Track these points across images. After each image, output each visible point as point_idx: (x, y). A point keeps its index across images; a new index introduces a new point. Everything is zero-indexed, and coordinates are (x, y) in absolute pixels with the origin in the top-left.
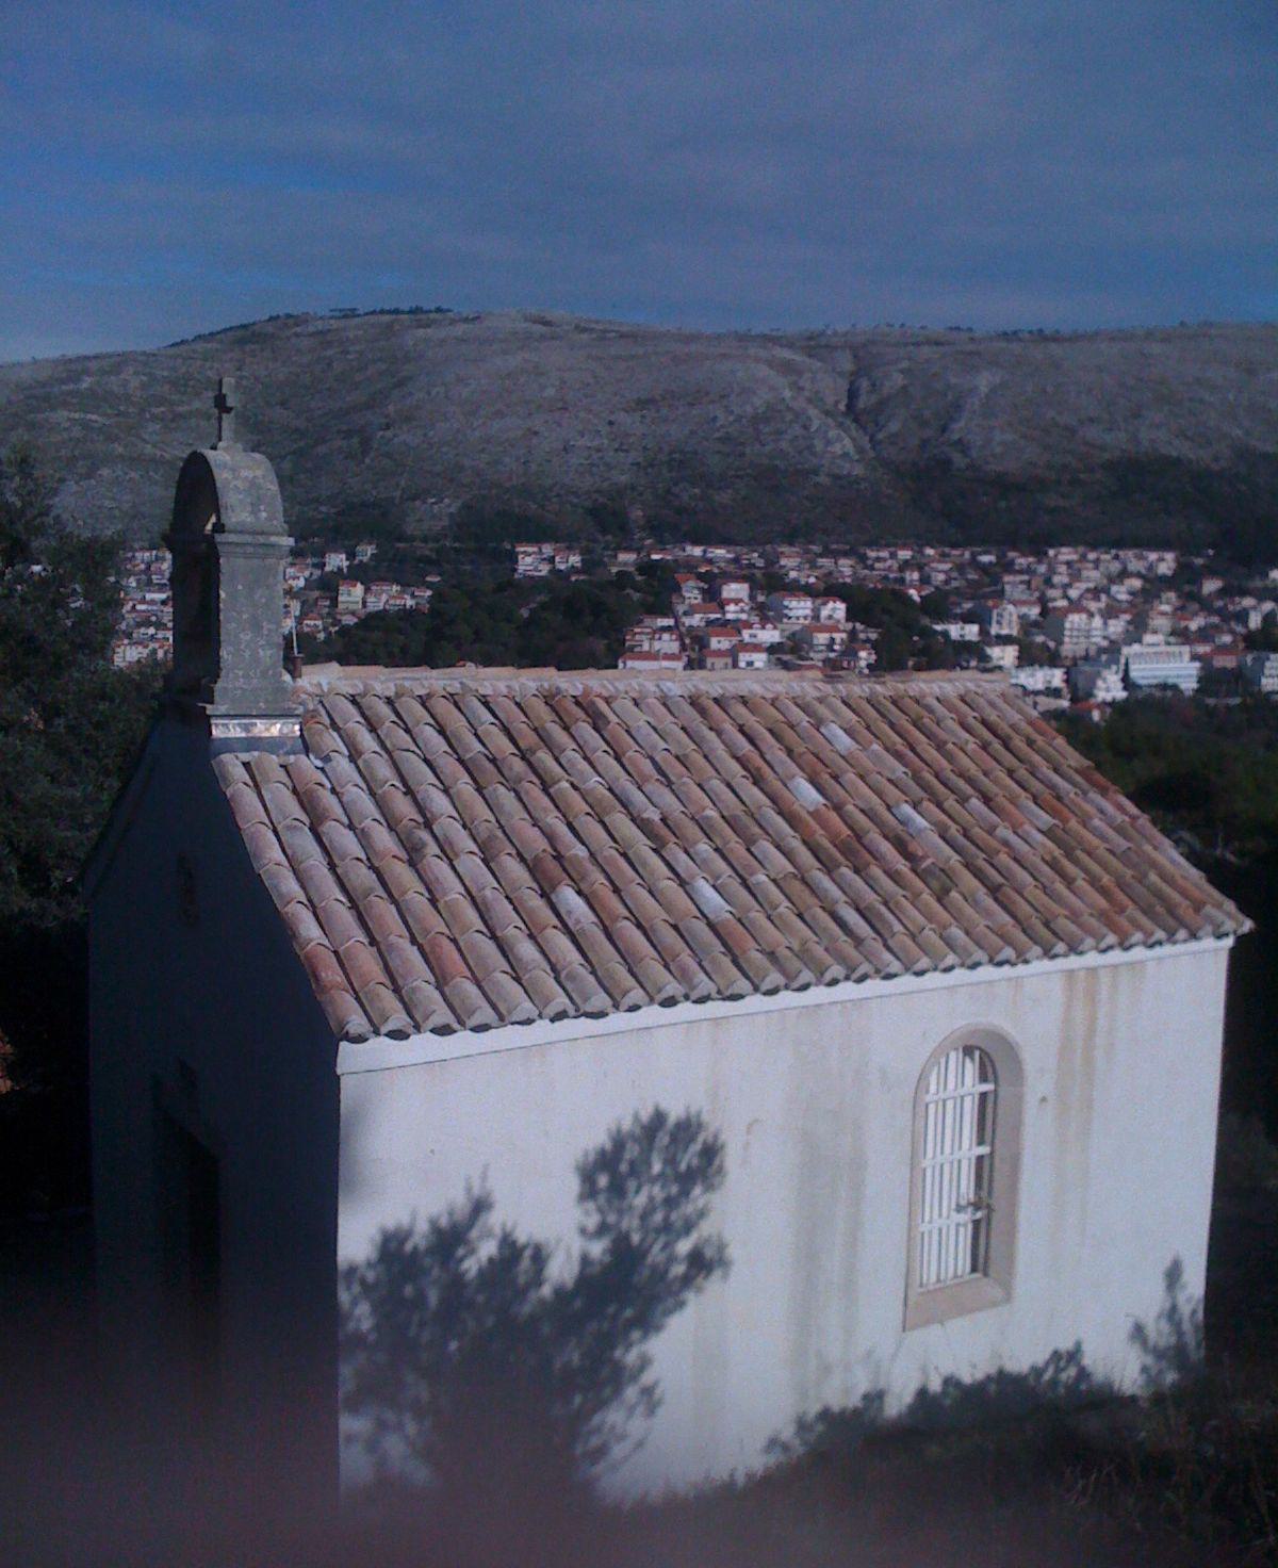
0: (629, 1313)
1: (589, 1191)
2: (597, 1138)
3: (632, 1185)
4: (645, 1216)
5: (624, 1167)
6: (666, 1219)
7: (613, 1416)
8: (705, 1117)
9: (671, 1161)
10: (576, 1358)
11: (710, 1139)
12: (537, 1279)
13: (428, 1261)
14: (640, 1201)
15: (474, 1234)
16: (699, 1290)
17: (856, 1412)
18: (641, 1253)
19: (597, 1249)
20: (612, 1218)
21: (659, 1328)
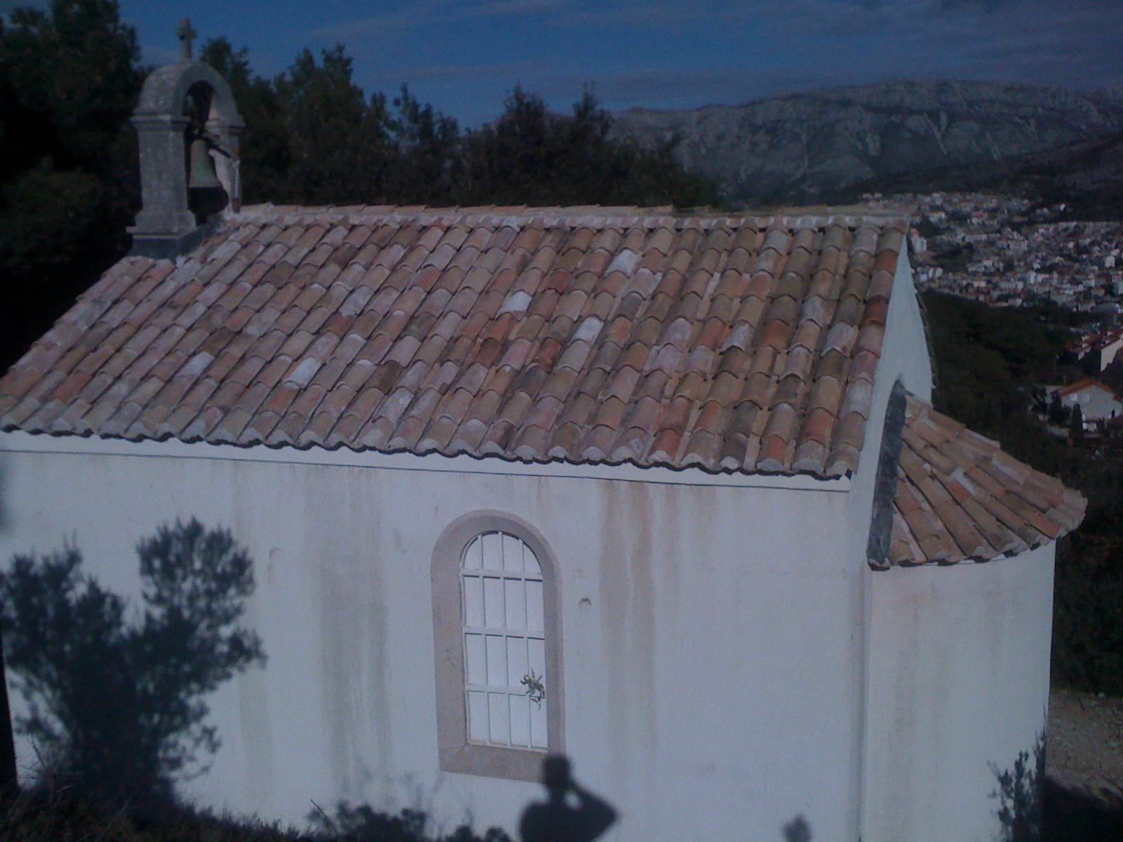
0: (187, 668)
1: (147, 570)
2: (150, 532)
3: (179, 573)
4: (192, 598)
5: (172, 558)
6: (209, 606)
7: (184, 741)
8: (235, 536)
9: (208, 563)
10: (151, 687)
11: (240, 555)
12: (117, 621)
13: (45, 585)
14: (187, 586)
15: (72, 575)
16: (242, 669)
17: (395, 820)
18: (190, 628)
19: (158, 612)
20: (166, 593)
21: (212, 688)
